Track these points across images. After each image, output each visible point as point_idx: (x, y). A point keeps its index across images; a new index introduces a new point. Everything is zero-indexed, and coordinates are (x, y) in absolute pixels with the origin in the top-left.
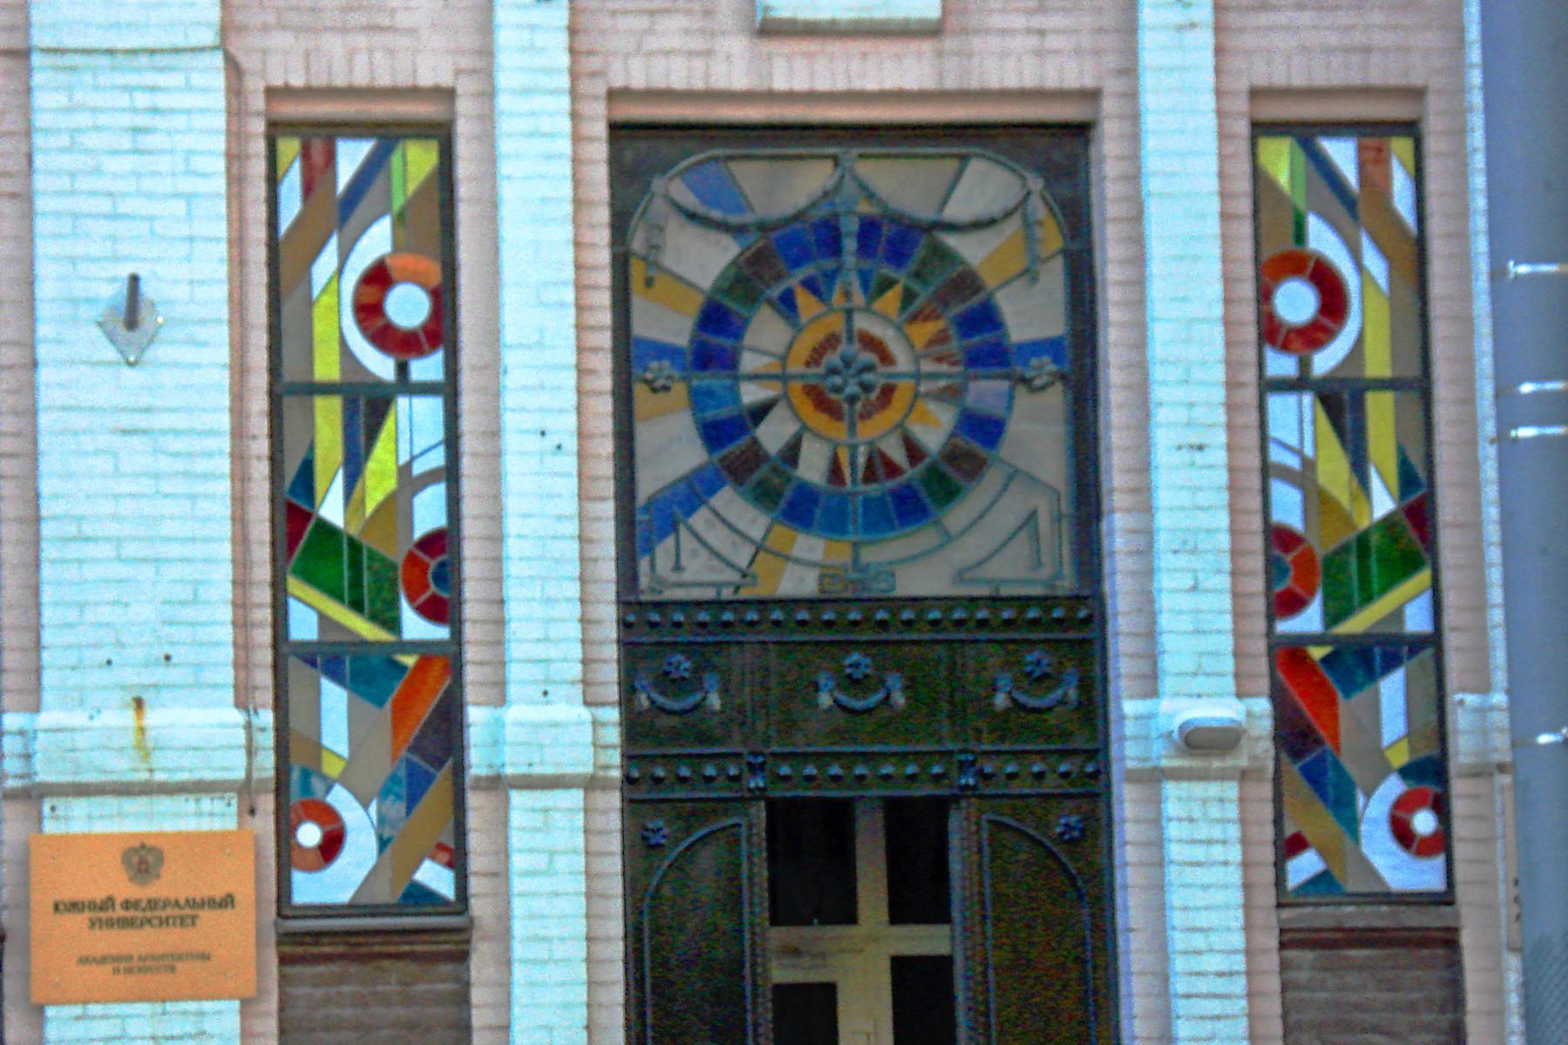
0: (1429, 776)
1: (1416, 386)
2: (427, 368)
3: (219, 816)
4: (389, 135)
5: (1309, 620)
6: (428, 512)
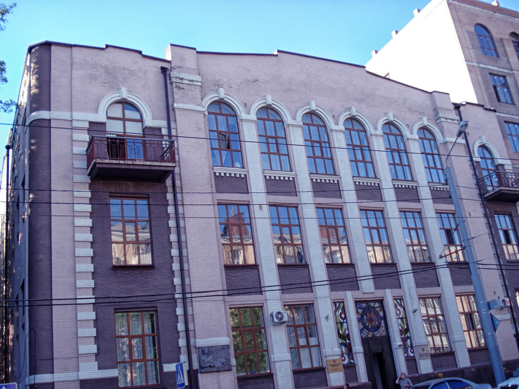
0: (412, 347)
1: (406, 318)
2: (345, 321)
3: (338, 357)
4: (340, 302)
5: (403, 336)
6: (347, 332)
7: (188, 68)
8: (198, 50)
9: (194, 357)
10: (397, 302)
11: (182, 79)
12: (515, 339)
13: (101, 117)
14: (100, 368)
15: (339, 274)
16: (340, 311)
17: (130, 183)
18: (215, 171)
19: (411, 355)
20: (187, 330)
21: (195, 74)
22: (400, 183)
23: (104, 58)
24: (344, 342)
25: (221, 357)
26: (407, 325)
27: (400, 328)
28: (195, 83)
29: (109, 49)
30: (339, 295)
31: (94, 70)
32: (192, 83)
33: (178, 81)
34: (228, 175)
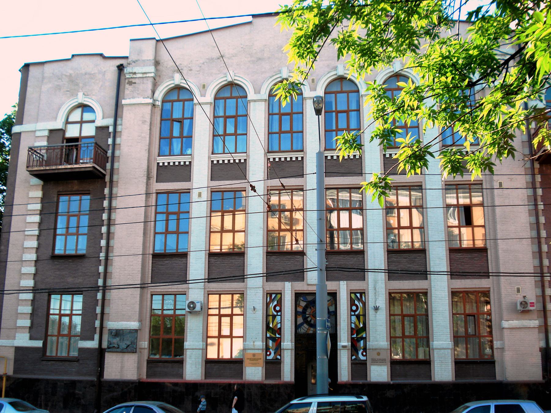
1: (364, 315)
2: (279, 314)
3: (260, 352)
4: (277, 294)
5: (355, 336)
6: (279, 326)
7: (144, 61)
8: (158, 38)
9: (105, 337)
10: (357, 296)
11: (135, 73)
12: (539, 354)
13: (58, 124)
14: (31, 338)
15: (404, 263)
16: (275, 303)
17: (76, 181)
18: (212, 159)
19: (362, 358)
20: (102, 313)
21: (150, 65)
22: (277, 156)
23: (68, 69)
24: (273, 336)
25: (127, 340)
26: (364, 324)
27: (353, 326)
28: (148, 75)
29: (76, 58)
30: (275, 286)
31: (60, 81)
32: (145, 76)
33: (131, 76)
34: (171, 164)
